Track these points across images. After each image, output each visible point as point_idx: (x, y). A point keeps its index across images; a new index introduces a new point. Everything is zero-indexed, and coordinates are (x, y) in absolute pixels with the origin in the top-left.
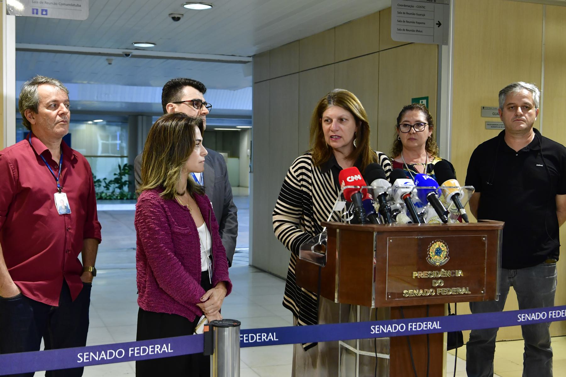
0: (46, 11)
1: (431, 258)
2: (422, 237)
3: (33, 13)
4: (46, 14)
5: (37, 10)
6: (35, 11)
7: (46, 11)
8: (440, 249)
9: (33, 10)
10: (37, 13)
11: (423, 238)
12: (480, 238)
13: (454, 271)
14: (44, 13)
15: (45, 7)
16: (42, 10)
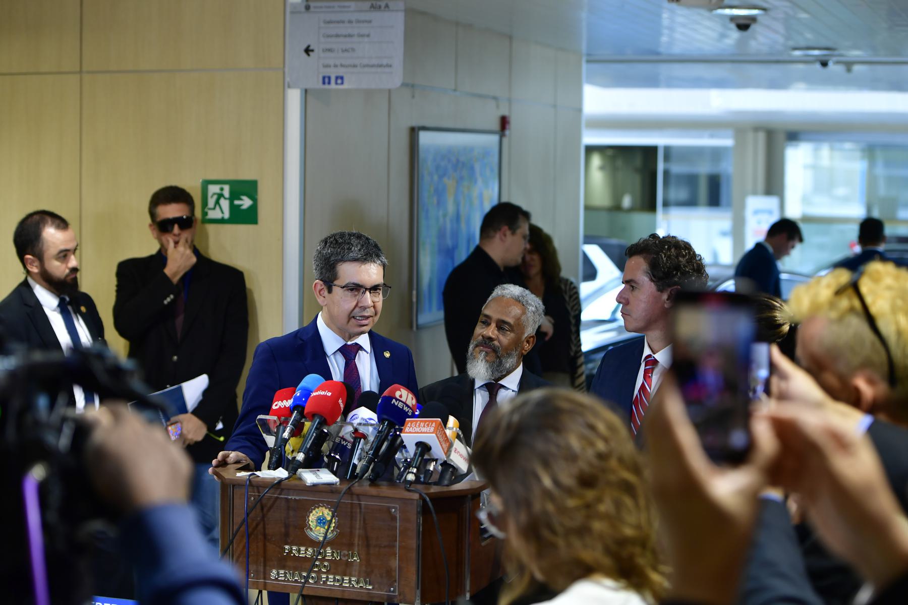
0: (342, 78)
1: (311, 529)
2: (297, 498)
3: (324, 83)
4: (342, 83)
5: (329, 78)
6: (327, 80)
7: (342, 78)
8: (324, 518)
9: (324, 78)
10: (329, 83)
11: (299, 500)
12: (389, 509)
13: (346, 553)
14: (339, 81)
15: (341, 72)
16: (337, 78)
